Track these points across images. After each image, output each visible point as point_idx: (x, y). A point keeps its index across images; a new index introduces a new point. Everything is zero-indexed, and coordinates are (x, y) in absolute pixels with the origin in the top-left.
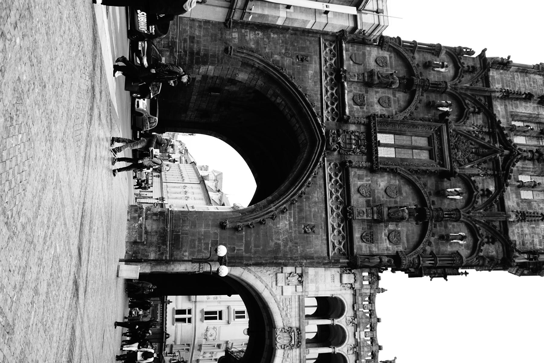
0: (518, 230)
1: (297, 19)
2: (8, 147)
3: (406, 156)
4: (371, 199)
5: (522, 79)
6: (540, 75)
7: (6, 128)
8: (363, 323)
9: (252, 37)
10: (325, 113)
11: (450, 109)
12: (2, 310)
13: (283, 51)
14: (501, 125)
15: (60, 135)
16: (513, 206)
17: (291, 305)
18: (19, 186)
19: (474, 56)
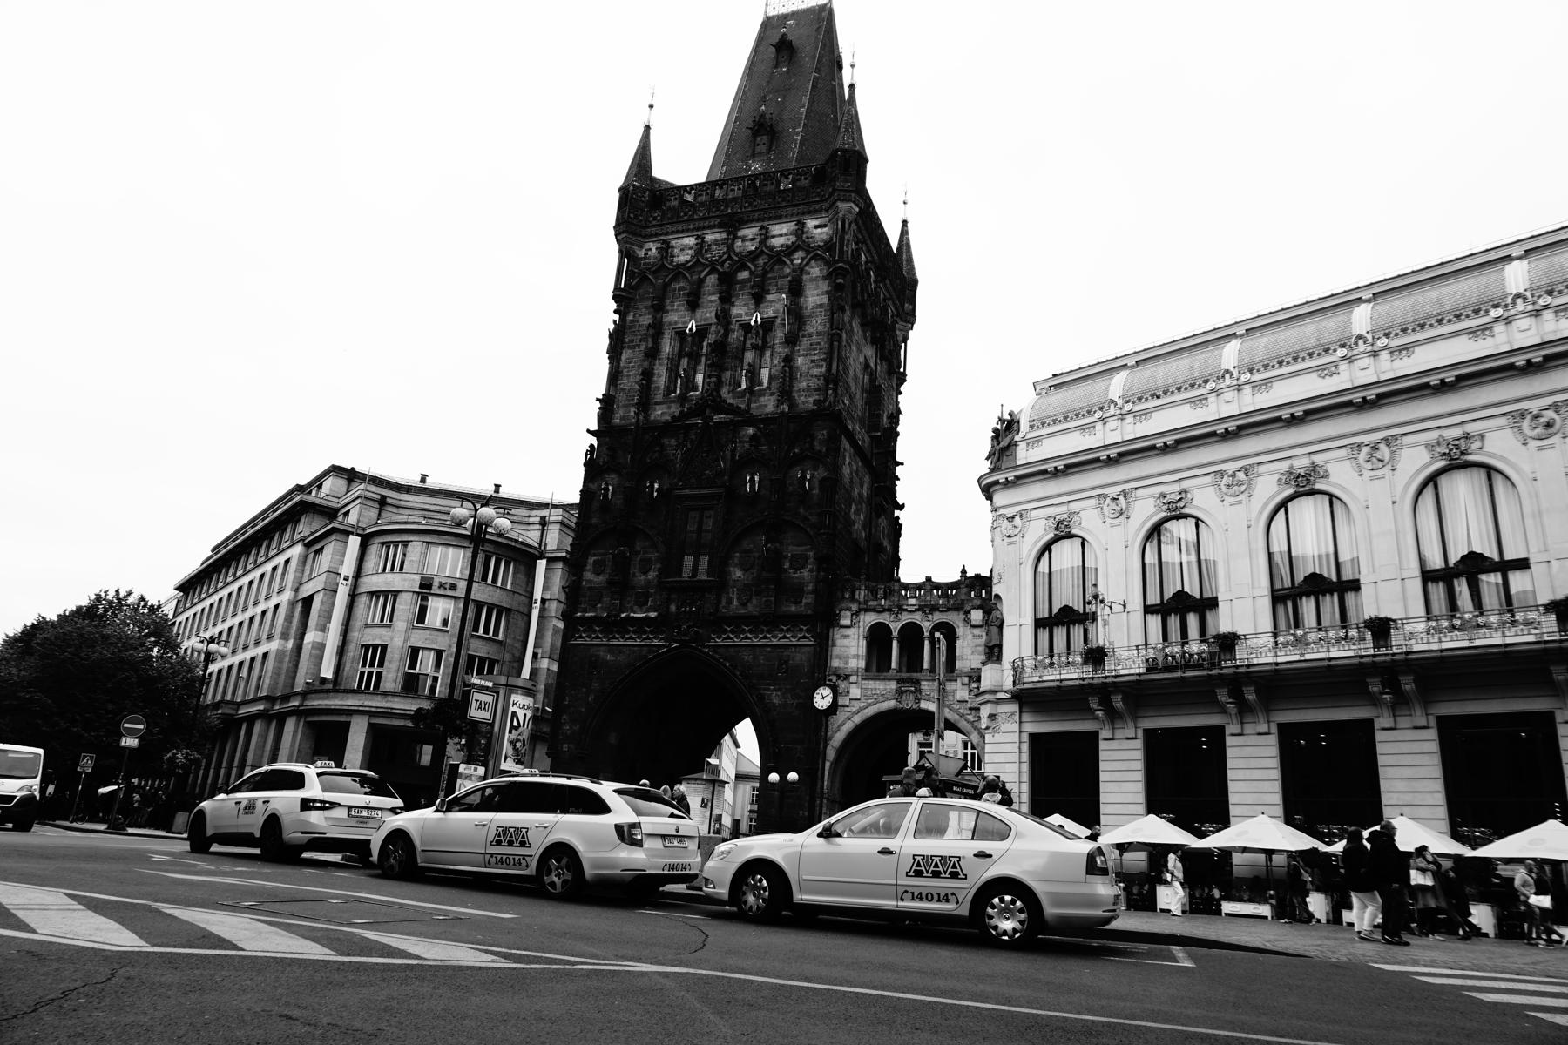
1: (551, 643)
4: (753, 589)
5: (625, 378)
6: (621, 355)
10: (656, 642)
13: (584, 690)
14: (677, 414)
19: (595, 444)
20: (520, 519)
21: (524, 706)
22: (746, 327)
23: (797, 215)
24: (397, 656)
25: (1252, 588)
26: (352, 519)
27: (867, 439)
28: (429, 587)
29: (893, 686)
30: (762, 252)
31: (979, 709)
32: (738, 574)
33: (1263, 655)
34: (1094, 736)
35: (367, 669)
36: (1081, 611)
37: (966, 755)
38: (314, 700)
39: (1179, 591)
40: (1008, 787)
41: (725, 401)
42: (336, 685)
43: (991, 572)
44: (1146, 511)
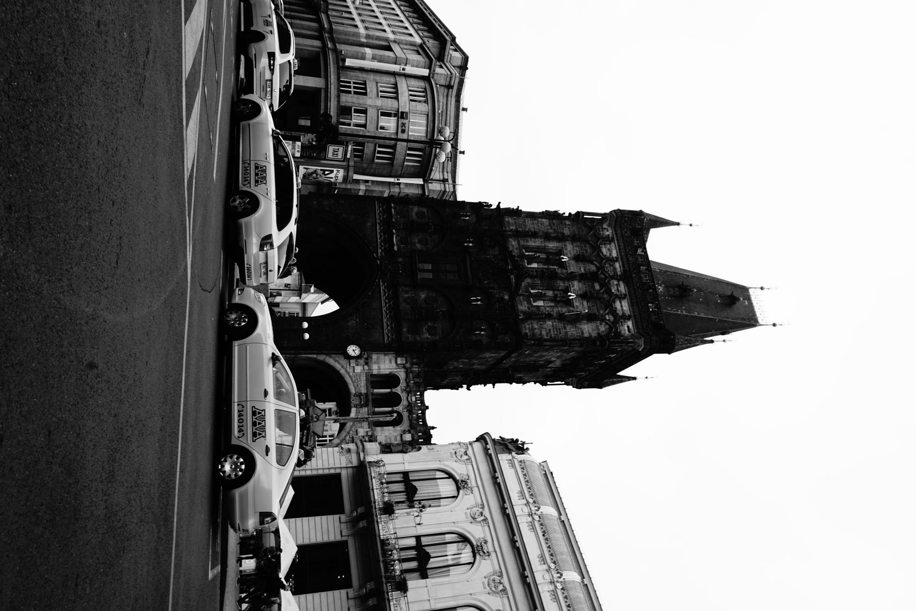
5: (532, 222)
6: (545, 218)
10: (379, 251)
14: (513, 254)
20: (445, 167)
21: (337, 177)
22: (567, 290)
23: (635, 315)
24: (361, 101)
25: (435, 599)
26: (438, 70)
27: (507, 365)
28: (402, 117)
29: (363, 391)
30: (611, 296)
31: (353, 442)
33: (396, 608)
34: (343, 512)
35: (352, 85)
36: (415, 499)
37: (326, 437)
38: (333, 56)
39: (430, 556)
40: (308, 463)
41: (523, 281)
42: (342, 68)
43: (434, 444)
44: (476, 532)
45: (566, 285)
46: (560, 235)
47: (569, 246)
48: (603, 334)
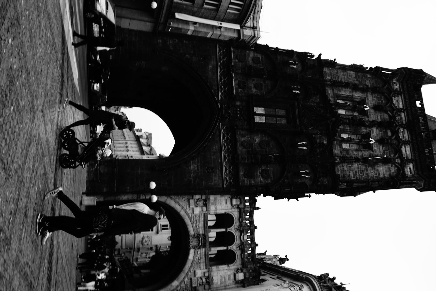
0: (341, 168)
2: (4, 115)
3: (272, 122)
5: (343, 73)
6: (353, 71)
7: (3, 102)
8: (245, 230)
9: (171, 43)
10: (220, 94)
11: (299, 92)
12: (2, 228)
13: (192, 52)
14: (331, 102)
15: (40, 108)
16: (338, 153)
17: (199, 220)
18: (12, 142)
19: (314, 58)
22: (368, 136)
30: (399, 143)
32: (257, 140)
45: (367, 131)
46: (365, 87)
47: (370, 97)
48: (393, 175)
